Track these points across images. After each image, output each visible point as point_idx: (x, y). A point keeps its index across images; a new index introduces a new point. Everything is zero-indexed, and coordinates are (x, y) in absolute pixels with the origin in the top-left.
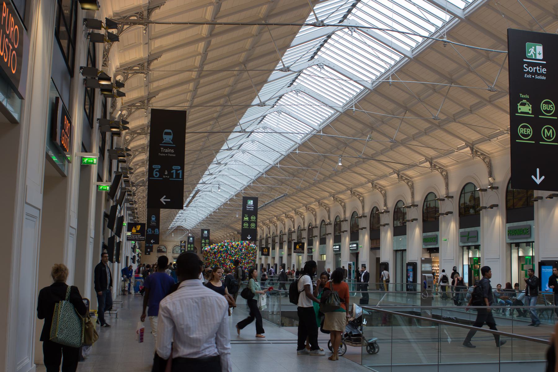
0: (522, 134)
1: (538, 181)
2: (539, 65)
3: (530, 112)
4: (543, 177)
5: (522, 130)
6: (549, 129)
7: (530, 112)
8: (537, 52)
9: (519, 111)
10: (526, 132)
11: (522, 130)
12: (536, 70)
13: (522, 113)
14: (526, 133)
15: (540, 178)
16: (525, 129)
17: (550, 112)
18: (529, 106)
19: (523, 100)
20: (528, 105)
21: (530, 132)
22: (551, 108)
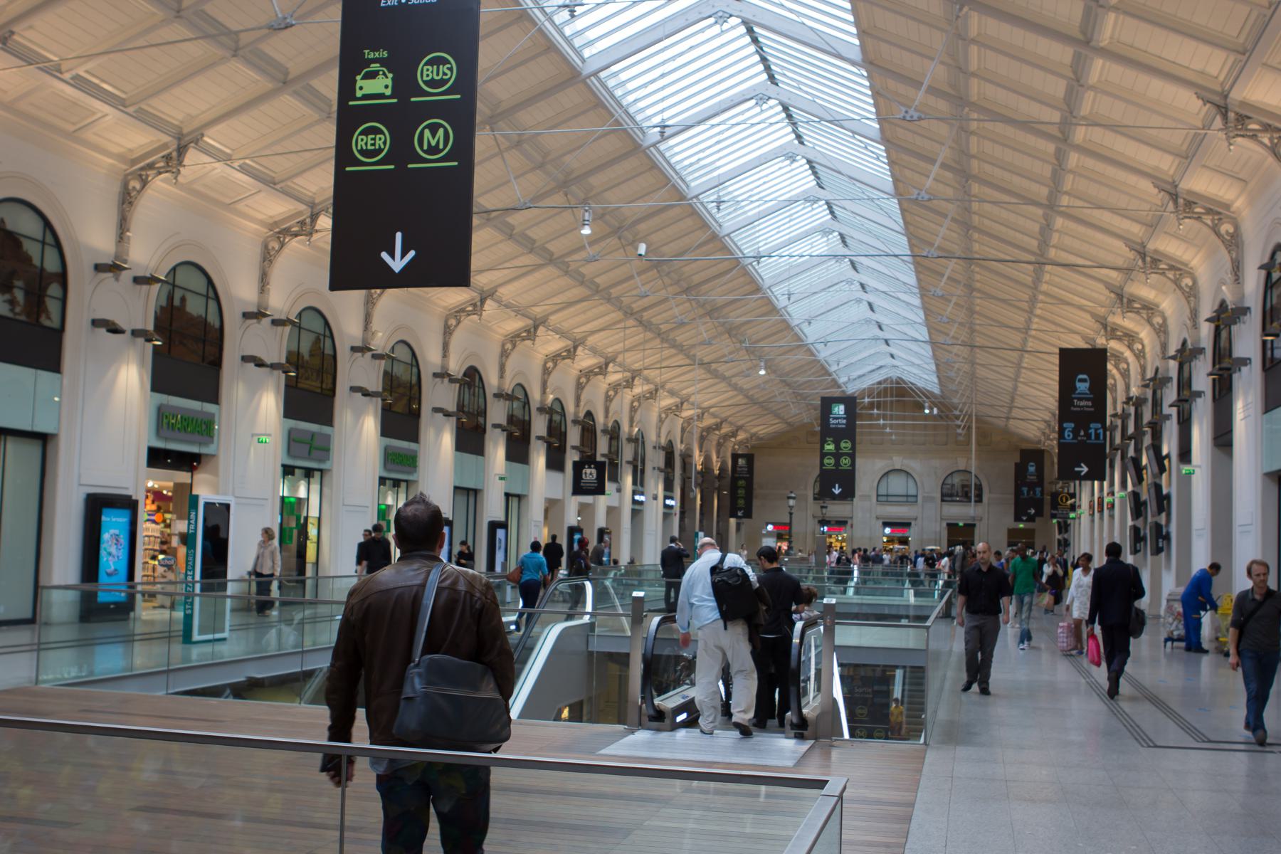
0: (362, 152)
1: (397, 264)
3: (388, 92)
4: (412, 254)
5: (362, 140)
6: (434, 129)
7: (388, 92)
10: (372, 145)
11: (362, 140)
13: (365, 97)
14: (373, 147)
15: (403, 256)
16: (370, 137)
17: (442, 82)
18: (387, 77)
19: (372, 65)
20: (384, 74)
21: (385, 143)
22: (445, 74)
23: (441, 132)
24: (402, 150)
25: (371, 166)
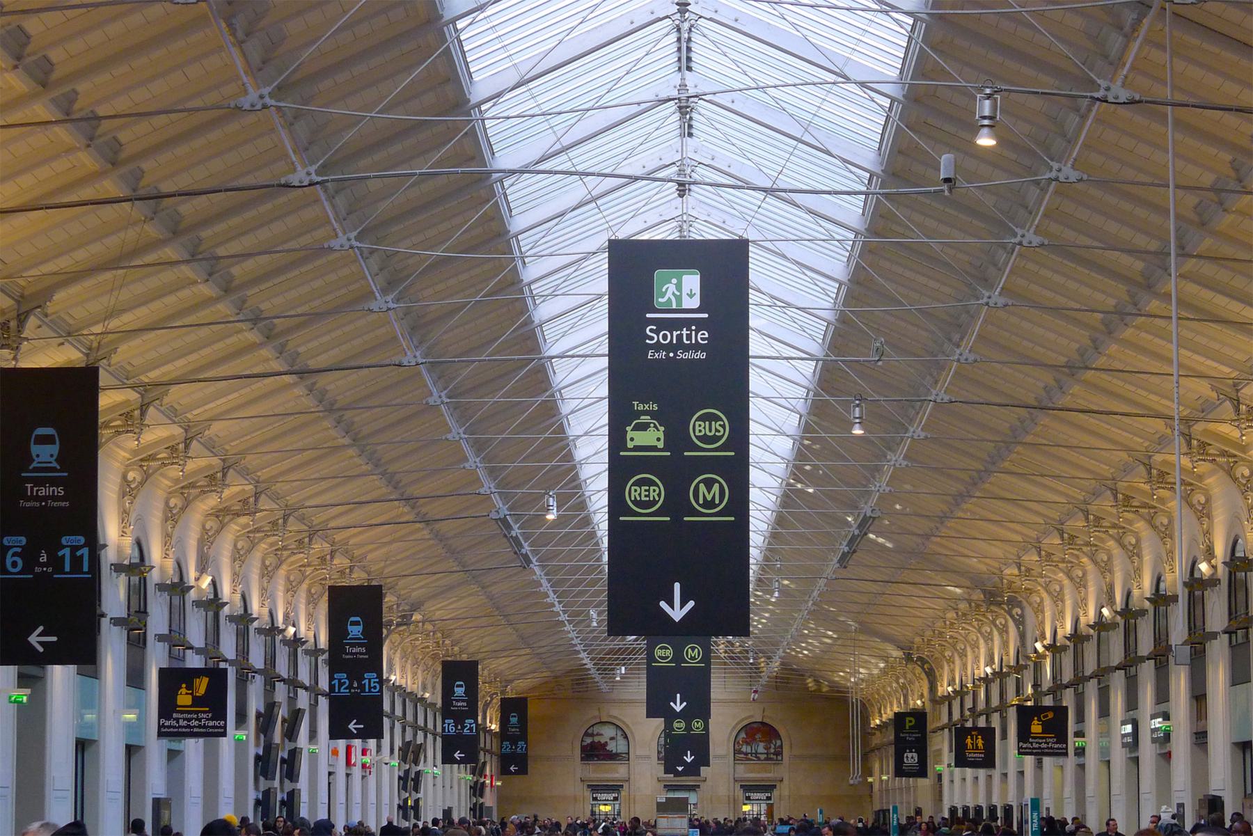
2: (687, 323)
3: (661, 445)
8: (685, 290)
9: (630, 445)
12: (680, 337)
13: (636, 448)
17: (715, 439)
23: (716, 487)
24: (677, 502)
25: (644, 516)
